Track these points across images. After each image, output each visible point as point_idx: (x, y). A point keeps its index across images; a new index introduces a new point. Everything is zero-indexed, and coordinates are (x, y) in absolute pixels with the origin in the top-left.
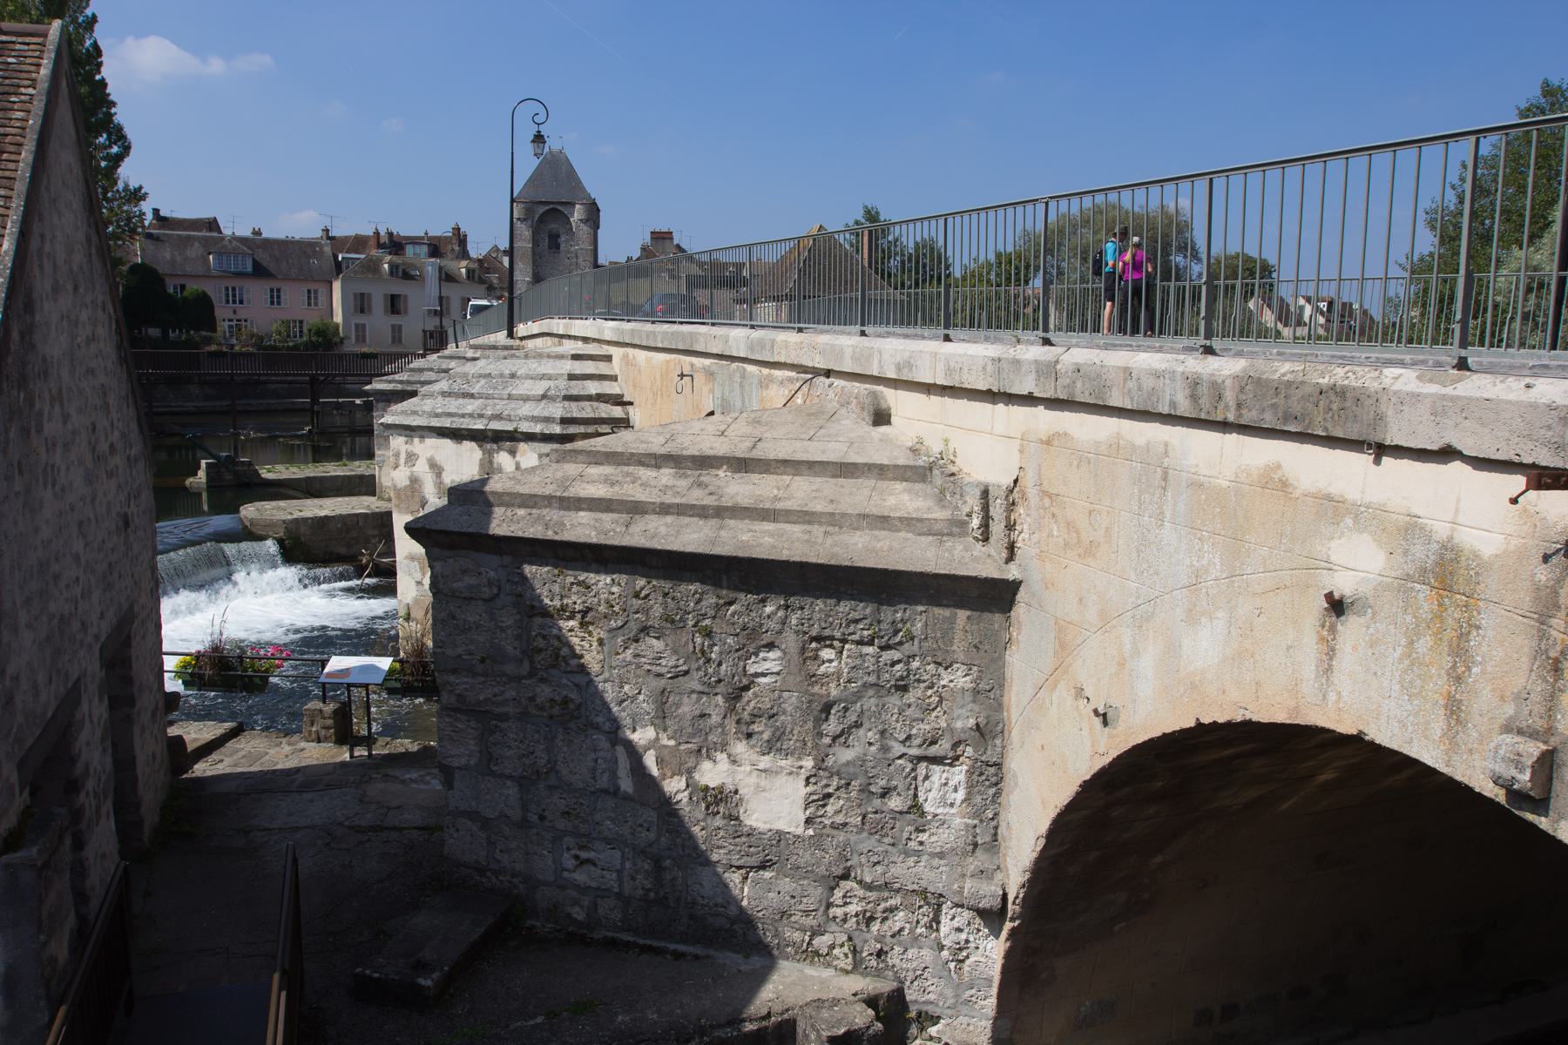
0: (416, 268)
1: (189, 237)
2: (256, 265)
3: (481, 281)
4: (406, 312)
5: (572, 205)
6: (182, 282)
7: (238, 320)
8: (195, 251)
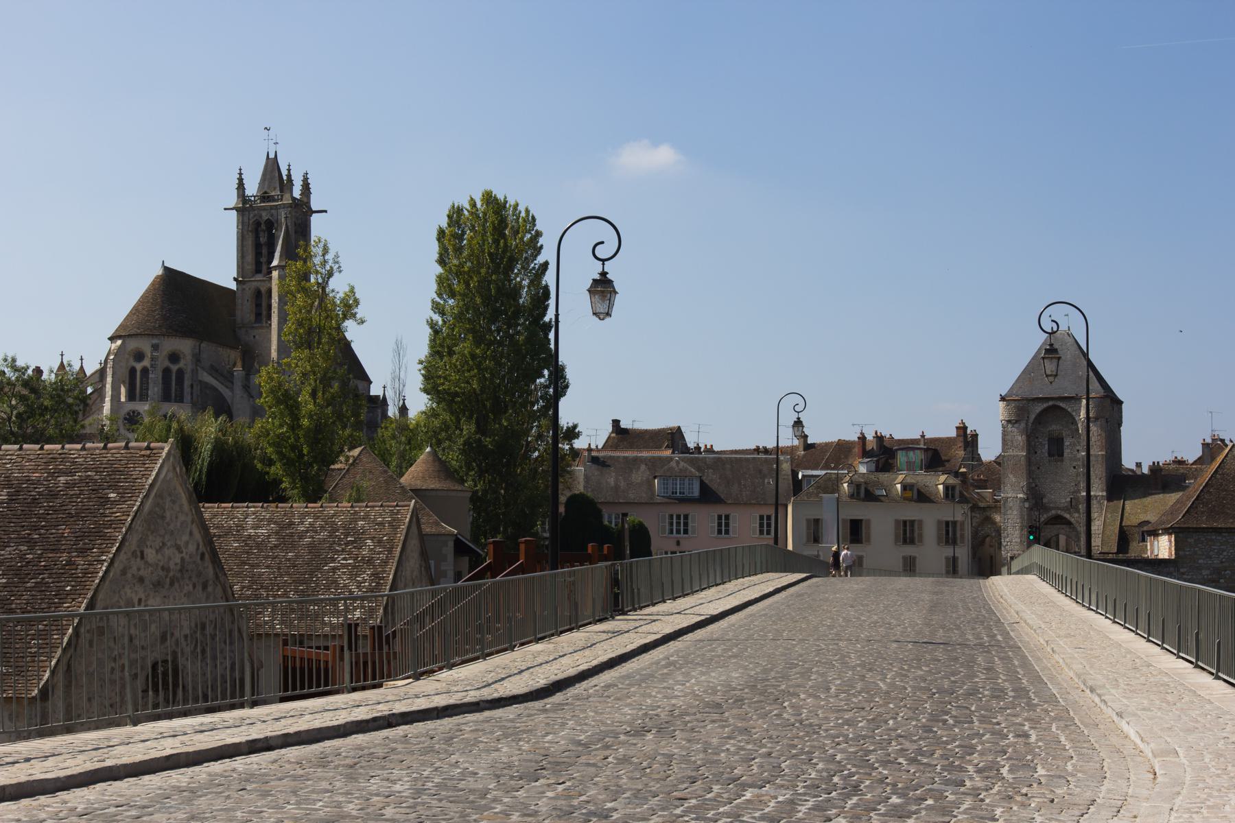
0: (880, 485)
1: (636, 459)
2: (703, 486)
3: (964, 500)
4: (868, 540)
5: (1075, 399)
8: (640, 475)
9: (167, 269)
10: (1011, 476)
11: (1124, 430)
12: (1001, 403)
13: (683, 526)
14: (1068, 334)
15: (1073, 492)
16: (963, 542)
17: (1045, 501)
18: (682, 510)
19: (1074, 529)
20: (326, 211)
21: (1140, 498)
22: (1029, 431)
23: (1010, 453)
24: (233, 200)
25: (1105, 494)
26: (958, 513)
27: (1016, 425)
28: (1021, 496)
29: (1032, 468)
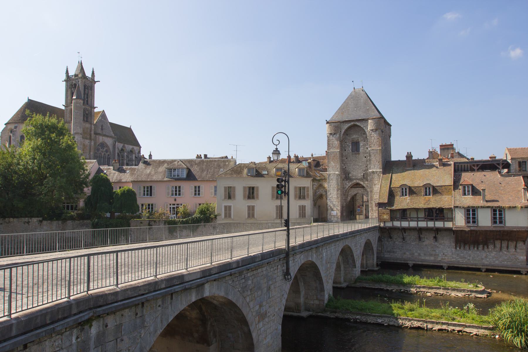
3: (308, 176)
4: (258, 198)
5: (365, 120)
6: (149, 185)
7: (177, 205)
9: (29, 100)
10: (332, 163)
11: (392, 139)
12: (327, 124)
13: (178, 191)
14: (362, 90)
15: (365, 170)
16: (308, 197)
17: (350, 175)
18: (178, 184)
19: (366, 190)
20: (99, 81)
21: (401, 173)
22: (341, 139)
23: (332, 150)
24: (64, 77)
25: (381, 170)
26: (307, 183)
27: (334, 136)
28: (337, 173)
29: (343, 159)
